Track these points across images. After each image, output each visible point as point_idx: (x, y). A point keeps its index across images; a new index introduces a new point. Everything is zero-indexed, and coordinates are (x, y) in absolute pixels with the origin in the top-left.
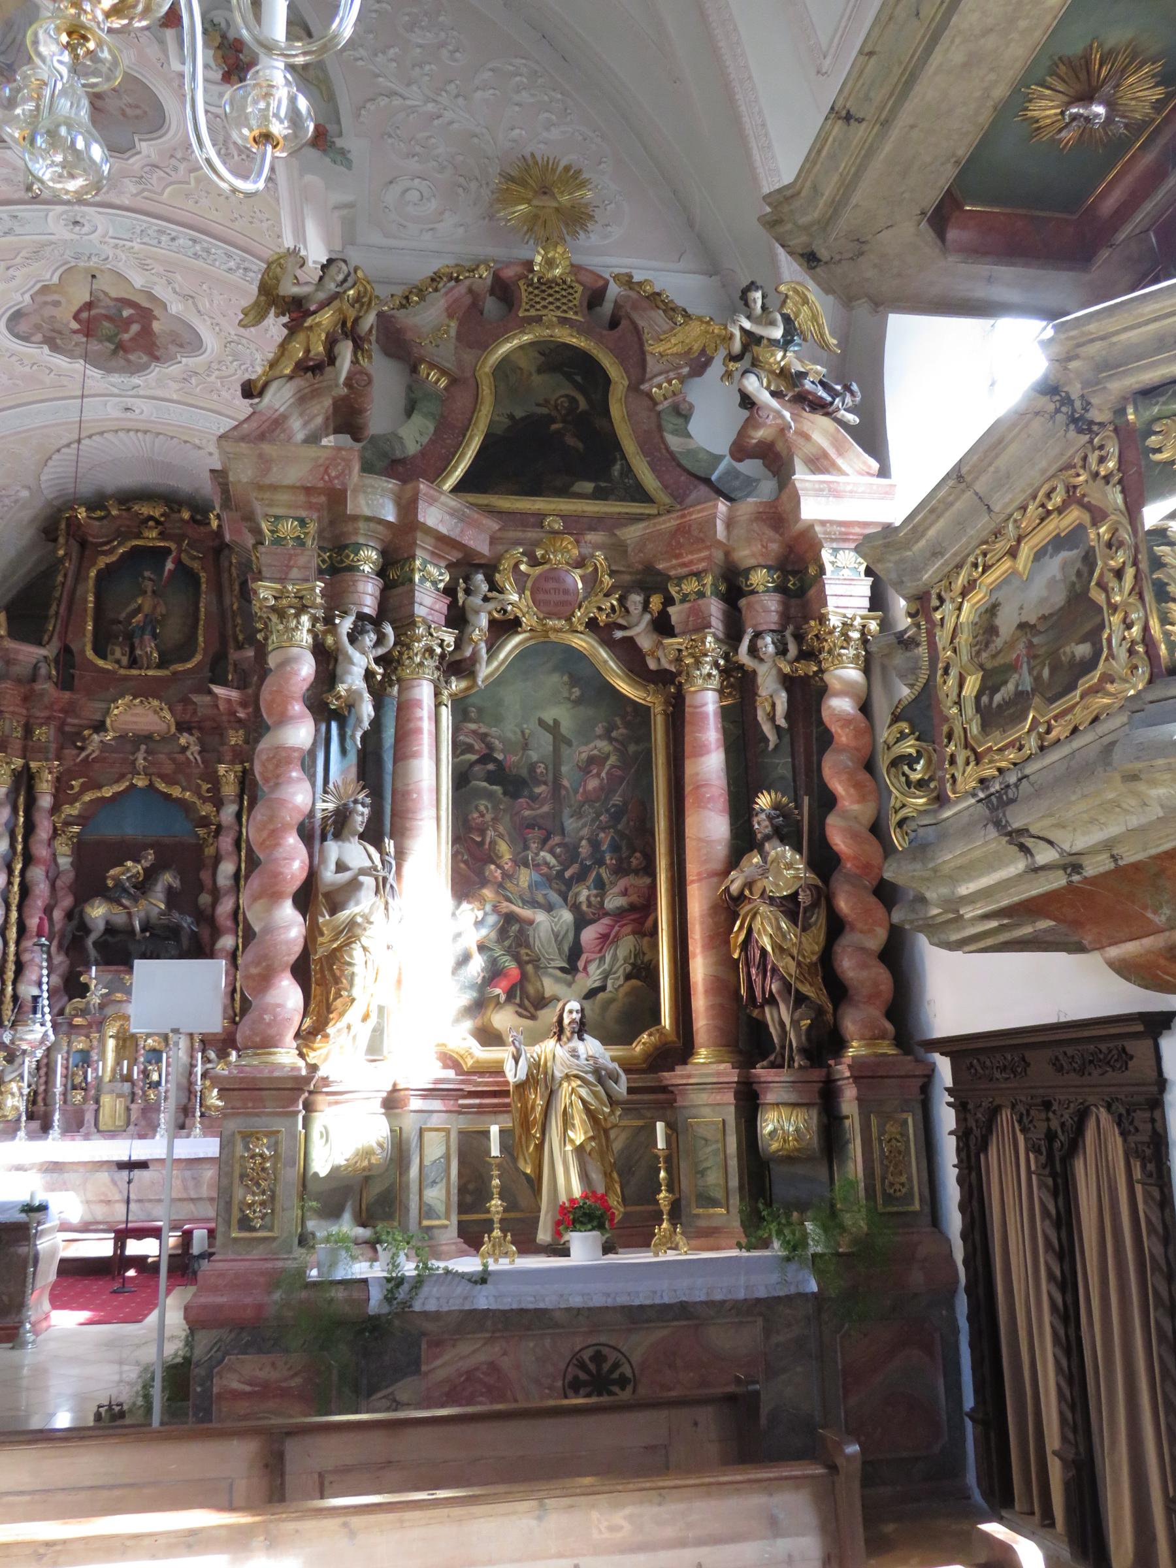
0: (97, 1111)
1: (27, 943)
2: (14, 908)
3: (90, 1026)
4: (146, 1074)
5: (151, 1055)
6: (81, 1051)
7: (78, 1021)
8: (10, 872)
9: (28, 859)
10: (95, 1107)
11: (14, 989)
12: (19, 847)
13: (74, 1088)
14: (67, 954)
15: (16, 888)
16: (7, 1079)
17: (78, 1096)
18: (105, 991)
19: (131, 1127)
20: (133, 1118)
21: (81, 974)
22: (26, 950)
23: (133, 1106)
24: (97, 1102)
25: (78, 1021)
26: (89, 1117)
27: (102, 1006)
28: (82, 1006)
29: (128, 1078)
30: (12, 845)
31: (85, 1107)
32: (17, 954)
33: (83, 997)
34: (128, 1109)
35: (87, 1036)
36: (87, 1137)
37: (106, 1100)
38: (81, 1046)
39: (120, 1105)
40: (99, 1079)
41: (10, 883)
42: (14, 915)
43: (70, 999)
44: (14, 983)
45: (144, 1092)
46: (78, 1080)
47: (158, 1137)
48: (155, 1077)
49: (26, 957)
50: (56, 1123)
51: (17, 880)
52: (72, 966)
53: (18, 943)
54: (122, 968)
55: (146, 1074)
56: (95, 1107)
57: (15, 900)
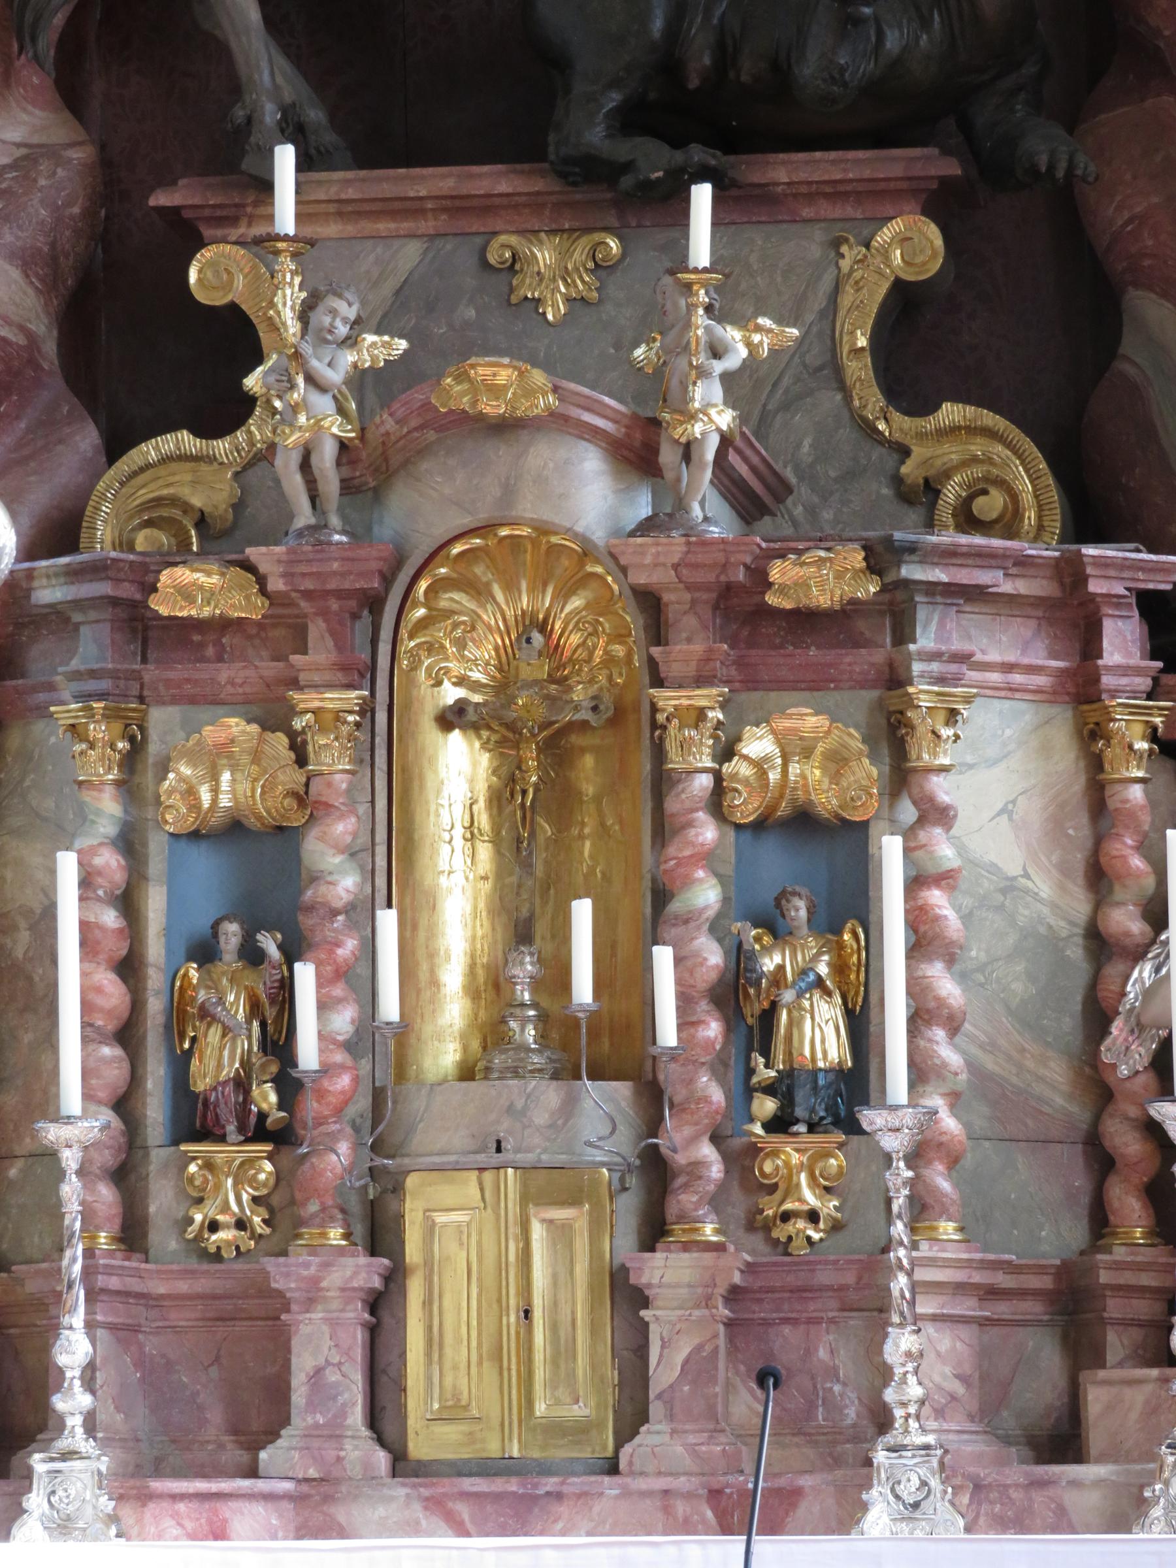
0: (382, 1307)
3: (283, 628)
4: (745, 1007)
5: (775, 862)
6: (234, 830)
7: (193, 588)
10: (363, 1271)
13: (195, 1122)
14: (71, 94)
17: (229, 1186)
18: (381, 348)
19: (654, 1437)
20: (665, 1368)
21: (186, 236)
23: (666, 1272)
24: (379, 1232)
25: (193, 588)
26: (323, 1351)
27: (368, 472)
28: (212, 494)
29: (610, 1046)
31: (285, 1275)
33: (225, 411)
34: (626, 1296)
35: (273, 715)
36: (316, 1510)
37: (446, 1217)
38: (225, 792)
39: (558, 1261)
40: (383, 1050)
43: (116, 446)
45: (742, 1160)
46: (219, 1059)
47: (879, 1515)
48: (821, 1036)
50: (72, 1403)
52: (114, 184)
54: (492, 180)
55: (745, 1007)
56: (363, 1271)
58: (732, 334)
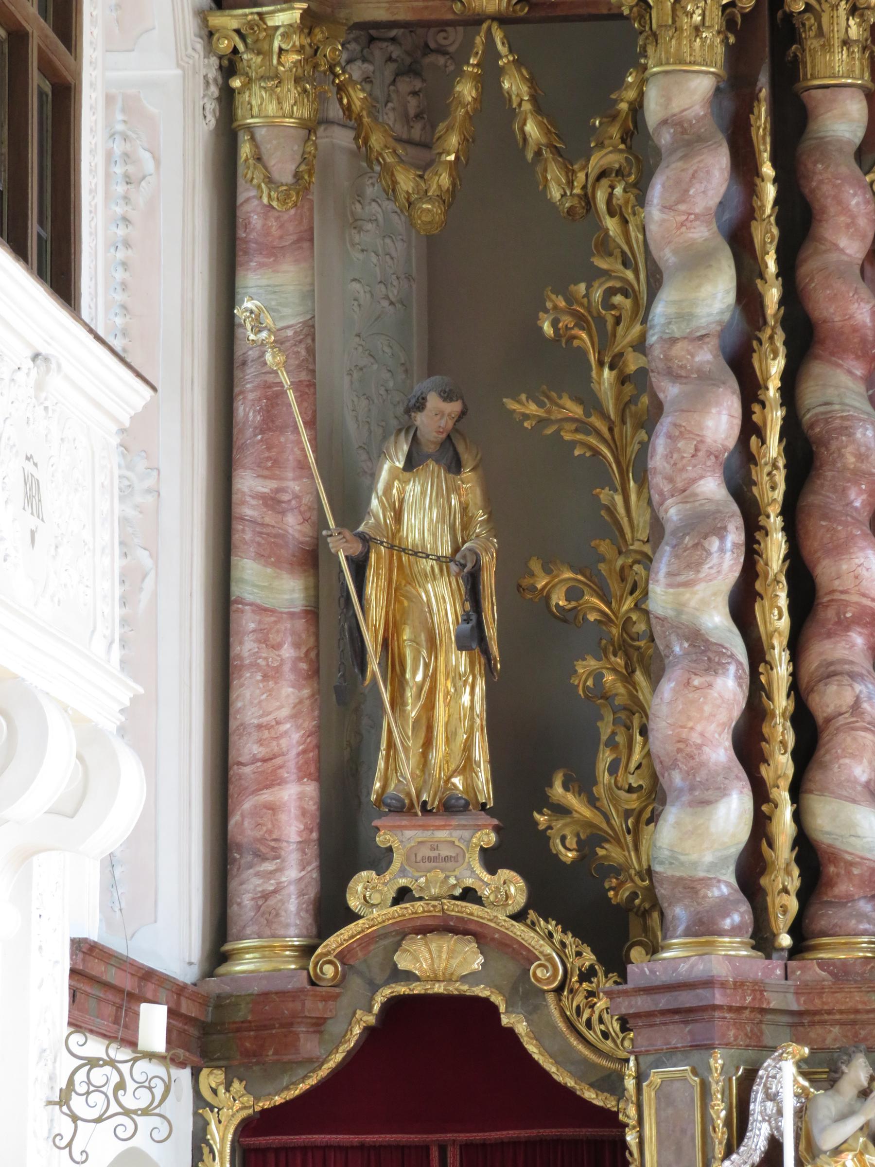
1: (824, 650)
2: (775, 521)
8: (750, 391)
9: (805, 338)
11: (797, 817)
12: (773, 295)
15: (774, 447)
16: (828, 1140)
22: (830, 673)
30: (748, 297)
32: (797, 689)
41: (750, 429)
42: (776, 548)
44: (796, 791)
49: (830, 700)
51: (774, 418)
53: (796, 646)
57: (772, 492)
58: (702, 590)
